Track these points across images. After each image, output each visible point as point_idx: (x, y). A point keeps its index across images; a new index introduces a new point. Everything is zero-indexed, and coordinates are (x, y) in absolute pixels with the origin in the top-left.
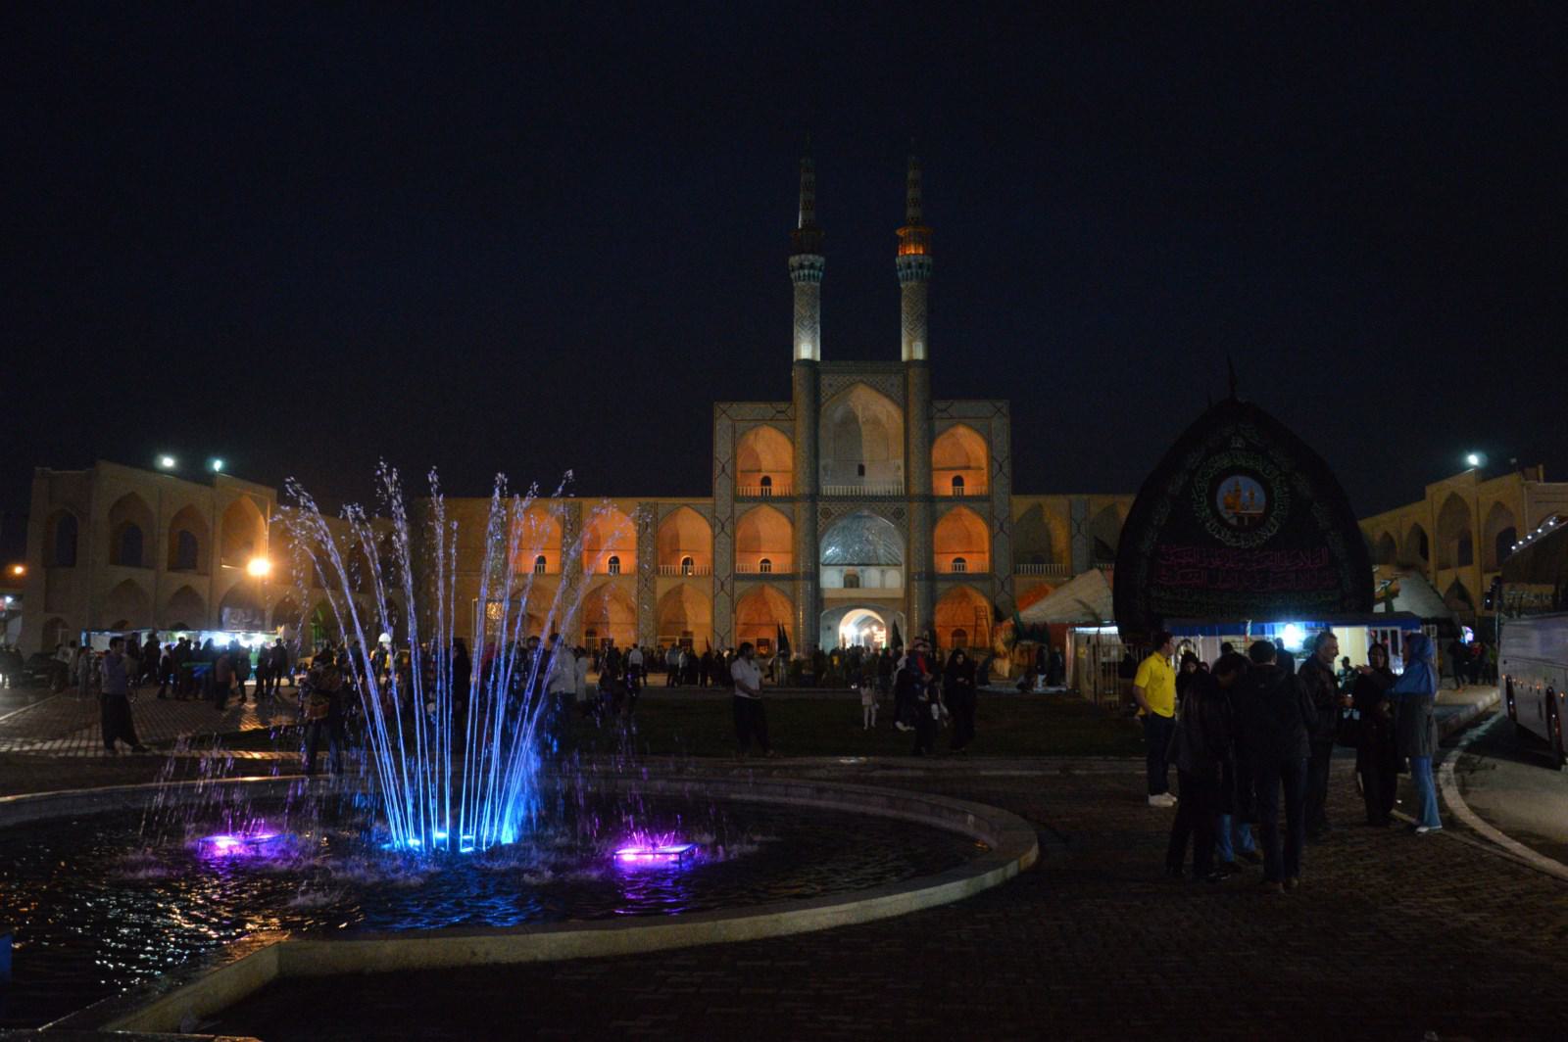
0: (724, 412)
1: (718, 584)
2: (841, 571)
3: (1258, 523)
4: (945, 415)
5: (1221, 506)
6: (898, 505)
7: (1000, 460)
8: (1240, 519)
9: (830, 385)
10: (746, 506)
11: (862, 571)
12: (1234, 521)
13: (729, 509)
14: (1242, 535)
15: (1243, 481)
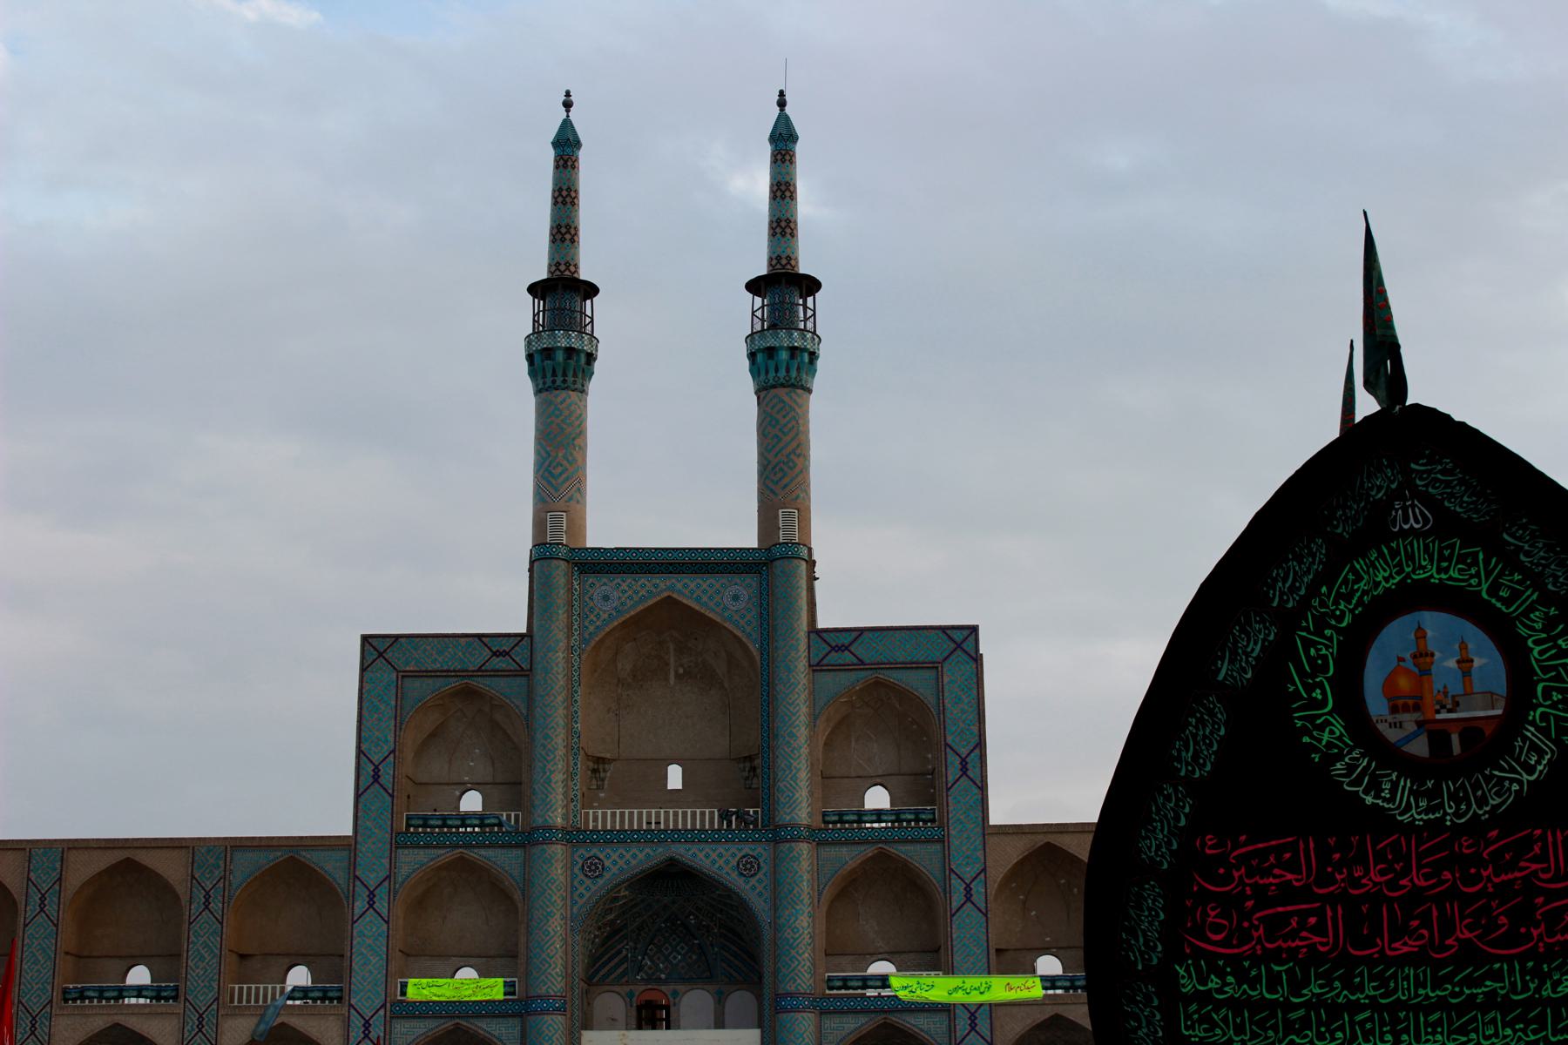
0: (381, 655)
1: (357, 1023)
2: (631, 995)
3: (1490, 744)
4: (847, 657)
5: (1377, 705)
6: (747, 849)
7: (964, 752)
8: (1438, 737)
9: (606, 598)
10: (422, 856)
11: (675, 993)
12: (1420, 748)
13: (386, 862)
14: (1448, 786)
15: (1436, 624)
